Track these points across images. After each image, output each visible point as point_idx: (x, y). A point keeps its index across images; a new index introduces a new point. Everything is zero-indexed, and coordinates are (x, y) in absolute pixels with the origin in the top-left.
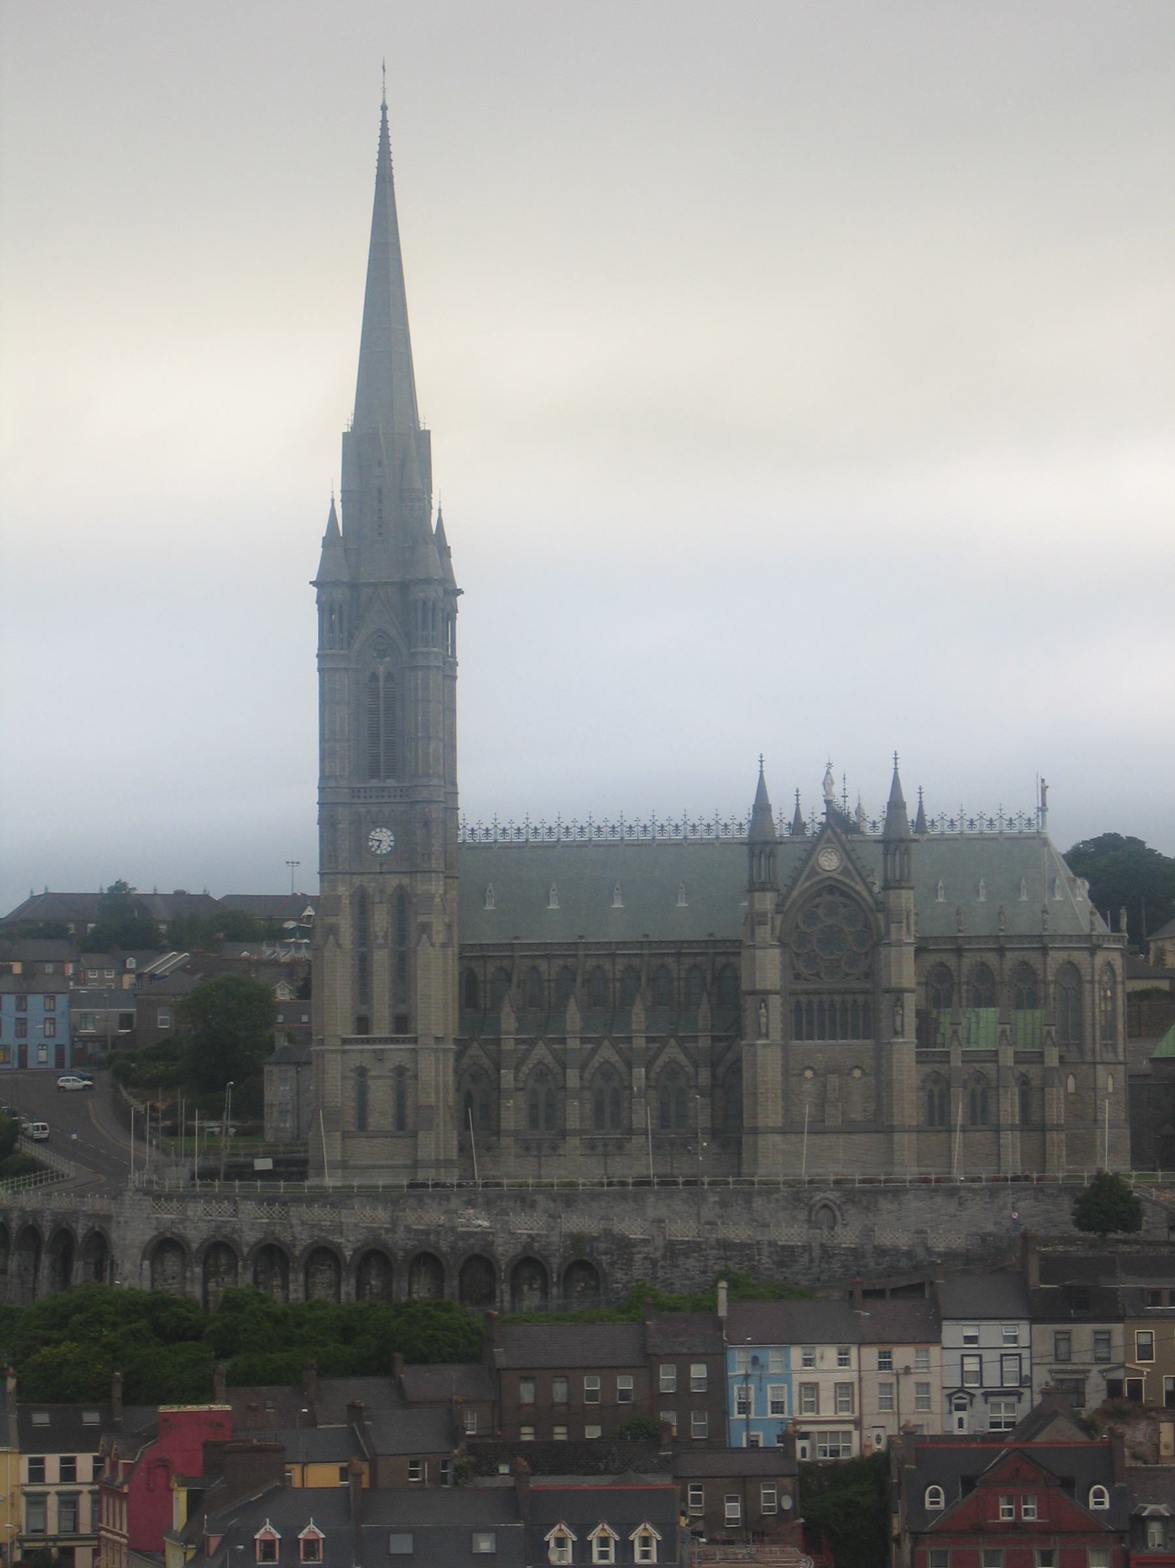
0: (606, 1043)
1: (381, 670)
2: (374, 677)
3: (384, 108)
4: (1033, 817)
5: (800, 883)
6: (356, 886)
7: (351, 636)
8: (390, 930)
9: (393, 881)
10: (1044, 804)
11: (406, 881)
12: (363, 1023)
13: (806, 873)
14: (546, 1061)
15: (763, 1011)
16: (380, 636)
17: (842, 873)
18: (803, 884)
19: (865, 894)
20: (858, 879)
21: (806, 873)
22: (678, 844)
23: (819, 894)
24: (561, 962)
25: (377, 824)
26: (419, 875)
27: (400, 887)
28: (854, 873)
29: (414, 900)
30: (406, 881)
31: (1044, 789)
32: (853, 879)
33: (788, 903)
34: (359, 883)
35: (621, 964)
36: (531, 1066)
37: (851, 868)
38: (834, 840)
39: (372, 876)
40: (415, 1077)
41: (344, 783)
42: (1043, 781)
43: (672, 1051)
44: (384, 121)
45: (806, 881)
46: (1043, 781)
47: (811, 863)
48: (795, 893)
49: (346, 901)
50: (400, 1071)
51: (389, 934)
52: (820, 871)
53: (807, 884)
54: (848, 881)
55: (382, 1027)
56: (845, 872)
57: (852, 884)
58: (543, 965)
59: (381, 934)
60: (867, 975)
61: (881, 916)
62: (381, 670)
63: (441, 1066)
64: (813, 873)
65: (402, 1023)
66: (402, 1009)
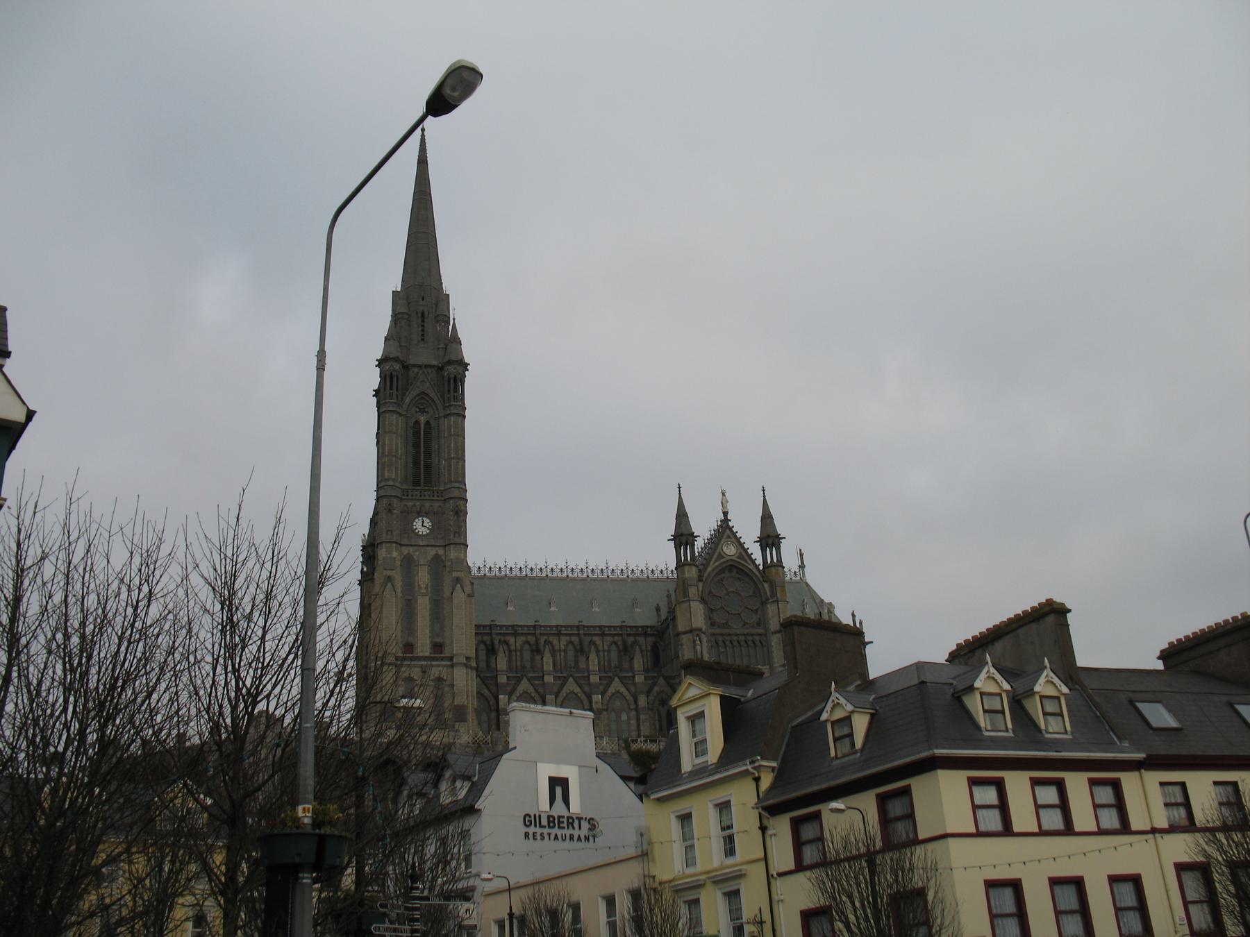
0: (571, 680)
1: (422, 419)
2: (417, 422)
4: (797, 571)
5: (712, 563)
6: (405, 554)
7: (404, 395)
8: (429, 584)
9: (432, 552)
10: (802, 562)
11: (441, 552)
12: (409, 647)
13: (715, 557)
14: (529, 691)
15: (698, 642)
16: (422, 398)
17: (738, 558)
18: (714, 563)
19: (754, 570)
20: (749, 562)
21: (715, 557)
22: (583, 580)
23: (722, 571)
24: (523, 638)
25: (419, 514)
26: (452, 546)
27: (437, 556)
28: (746, 558)
29: (448, 564)
30: (441, 552)
31: (801, 555)
32: (746, 561)
33: (706, 575)
34: (407, 552)
35: (564, 640)
36: (518, 695)
37: (744, 554)
38: (731, 536)
39: (416, 548)
40: (452, 686)
41: (398, 485)
42: (800, 550)
43: (617, 685)
45: (716, 561)
46: (800, 550)
47: (718, 551)
48: (709, 569)
49: (398, 563)
50: (439, 680)
51: (429, 587)
52: (725, 555)
53: (717, 564)
54: (743, 562)
56: (740, 557)
57: (746, 564)
58: (512, 640)
59: (423, 586)
60: (759, 624)
61: (766, 586)
62: (422, 419)
63: (470, 678)
64: (720, 556)
66: (438, 640)
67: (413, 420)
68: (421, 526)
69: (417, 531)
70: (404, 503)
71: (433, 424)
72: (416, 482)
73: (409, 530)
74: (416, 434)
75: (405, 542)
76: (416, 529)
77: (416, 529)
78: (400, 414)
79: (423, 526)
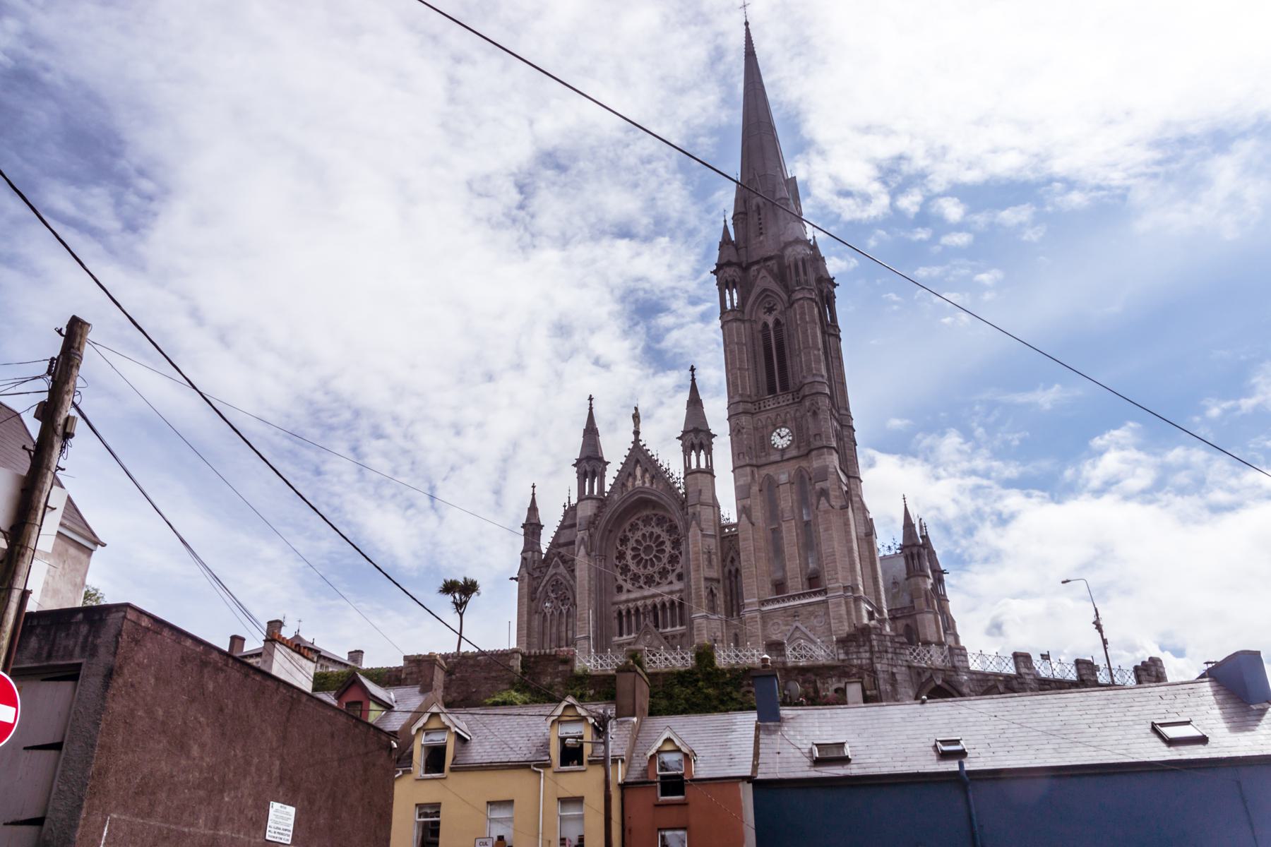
1: (770, 320)
2: (766, 325)
3: (747, 24)
16: (768, 296)
30: (804, 464)
44: (748, 30)
55: (796, 583)
65: (814, 582)
67: (761, 323)
68: (781, 439)
69: (776, 446)
70: (757, 418)
71: (783, 321)
72: (772, 390)
73: (765, 445)
74: (766, 338)
75: (763, 460)
76: (775, 443)
77: (775, 443)
78: (743, 321)
79: (782, 438)
